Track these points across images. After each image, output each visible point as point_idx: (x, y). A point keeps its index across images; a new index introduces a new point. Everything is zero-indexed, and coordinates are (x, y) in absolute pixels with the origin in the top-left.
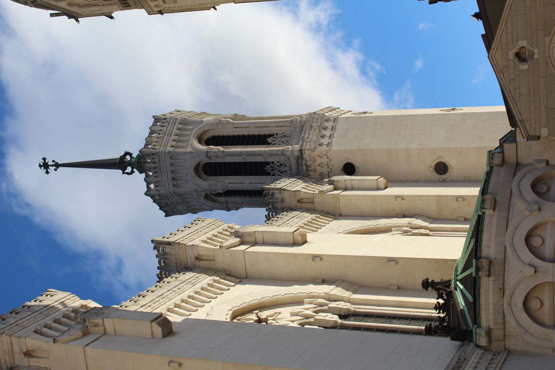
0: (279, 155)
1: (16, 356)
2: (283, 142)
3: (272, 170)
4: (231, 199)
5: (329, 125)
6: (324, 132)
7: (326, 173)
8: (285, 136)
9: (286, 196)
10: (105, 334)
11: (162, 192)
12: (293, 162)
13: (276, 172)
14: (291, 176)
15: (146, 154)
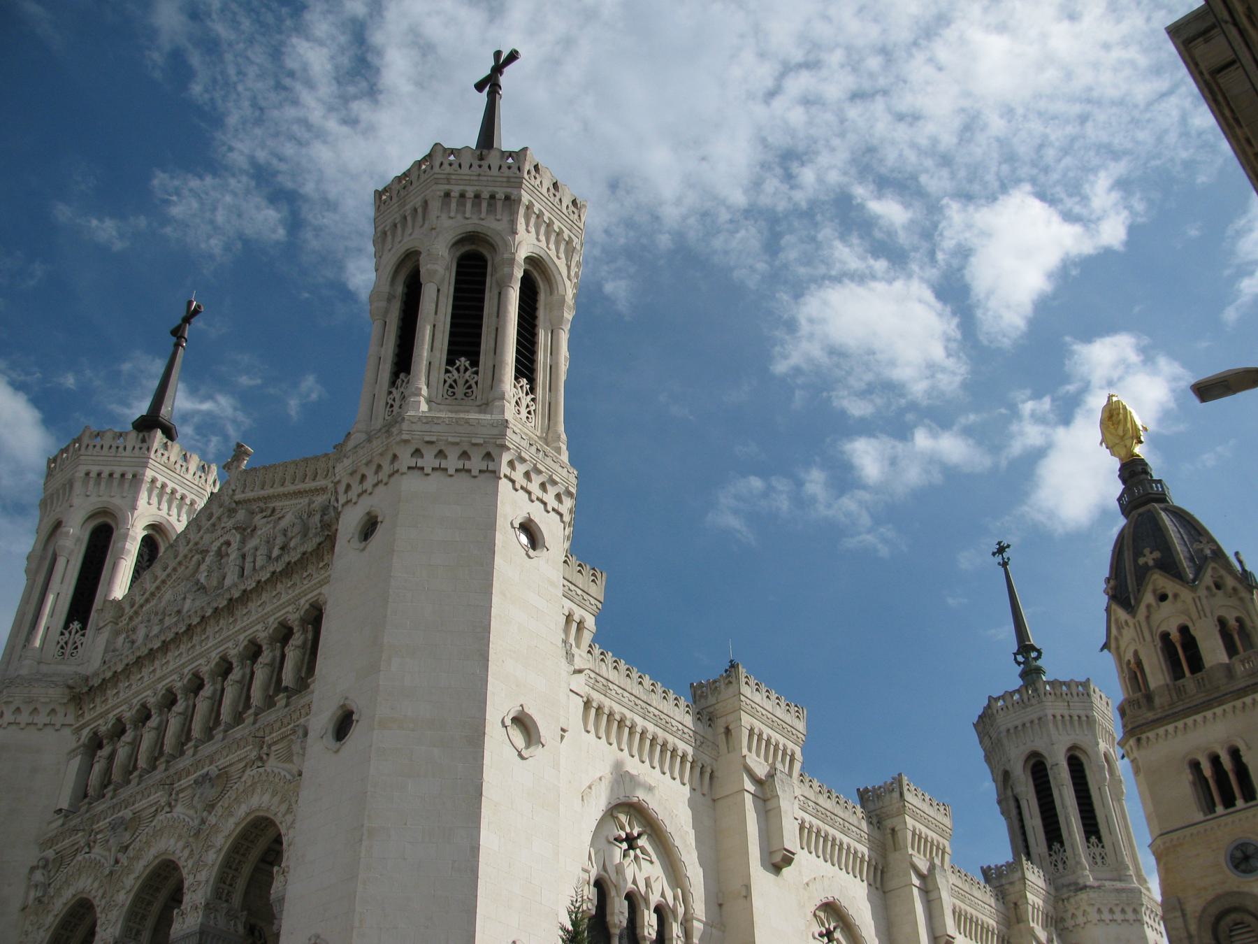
0: (1075, 858)
1: (723, 719)
2: (1094, 858)
3: (1055, 852)
4: (1012, 804)
5: (1130, 916)
6: (1117, 910)
7: (1066, 925)
8: (1103, 858)
9: (1018, 886)
10: (765, 801)
11: (998, 717)
12: (1070, 878)
13: (1055, 857)
14: (1050, 881)
15: (1037, 685)
